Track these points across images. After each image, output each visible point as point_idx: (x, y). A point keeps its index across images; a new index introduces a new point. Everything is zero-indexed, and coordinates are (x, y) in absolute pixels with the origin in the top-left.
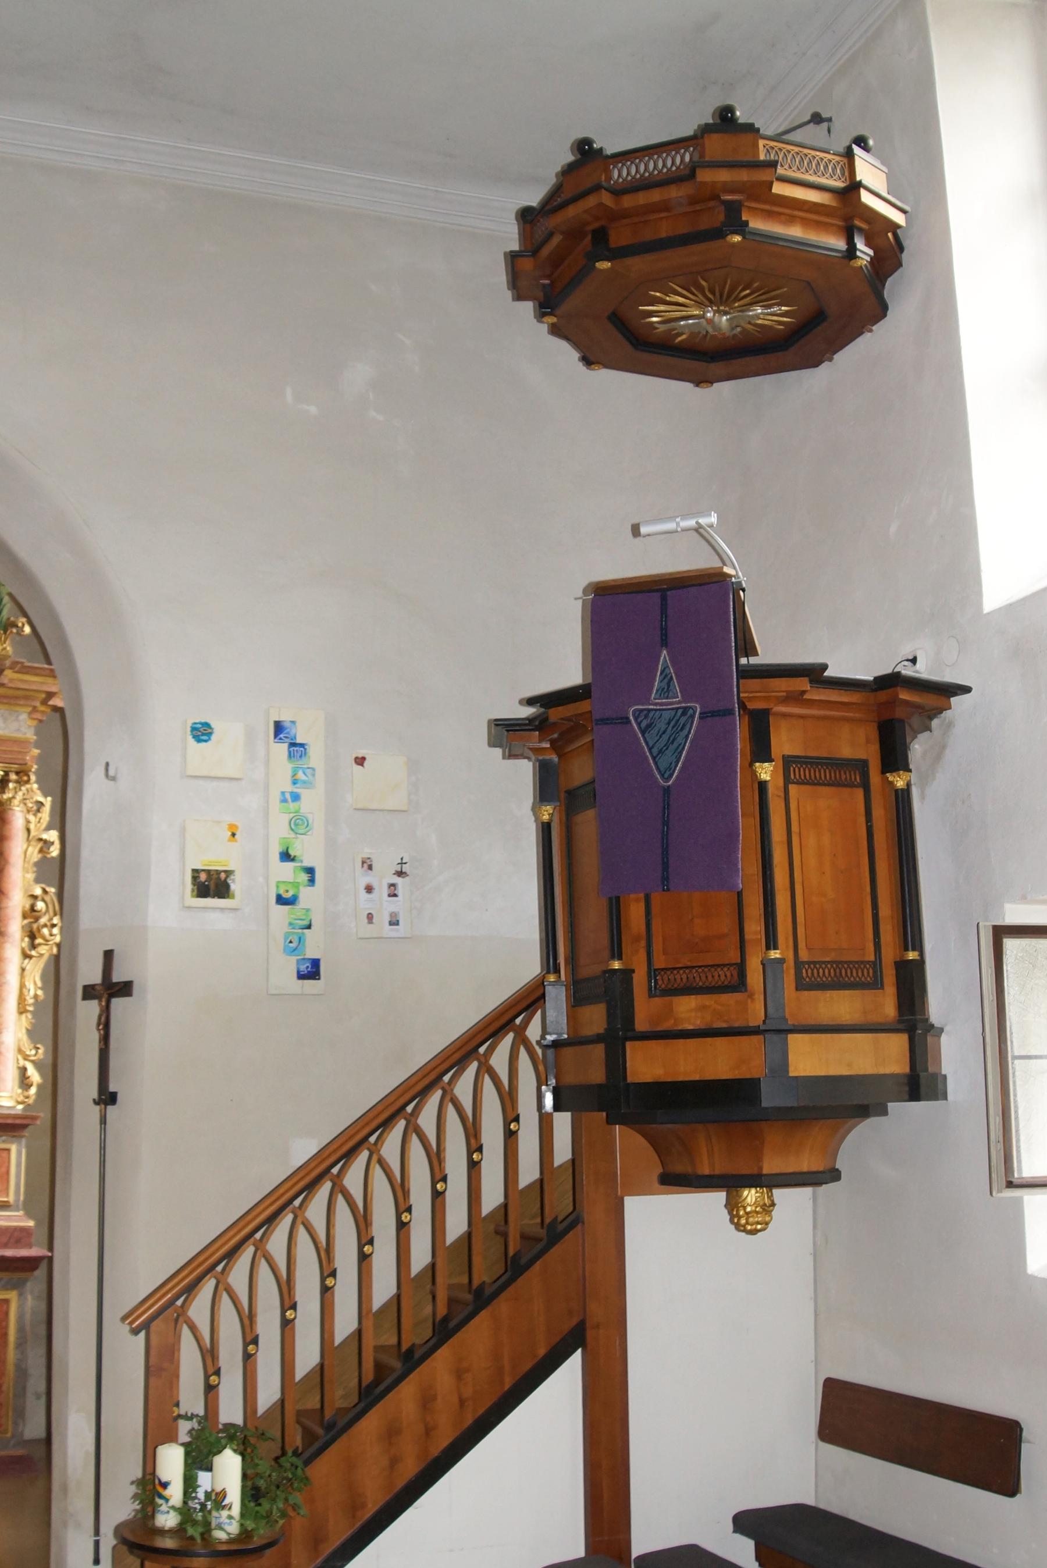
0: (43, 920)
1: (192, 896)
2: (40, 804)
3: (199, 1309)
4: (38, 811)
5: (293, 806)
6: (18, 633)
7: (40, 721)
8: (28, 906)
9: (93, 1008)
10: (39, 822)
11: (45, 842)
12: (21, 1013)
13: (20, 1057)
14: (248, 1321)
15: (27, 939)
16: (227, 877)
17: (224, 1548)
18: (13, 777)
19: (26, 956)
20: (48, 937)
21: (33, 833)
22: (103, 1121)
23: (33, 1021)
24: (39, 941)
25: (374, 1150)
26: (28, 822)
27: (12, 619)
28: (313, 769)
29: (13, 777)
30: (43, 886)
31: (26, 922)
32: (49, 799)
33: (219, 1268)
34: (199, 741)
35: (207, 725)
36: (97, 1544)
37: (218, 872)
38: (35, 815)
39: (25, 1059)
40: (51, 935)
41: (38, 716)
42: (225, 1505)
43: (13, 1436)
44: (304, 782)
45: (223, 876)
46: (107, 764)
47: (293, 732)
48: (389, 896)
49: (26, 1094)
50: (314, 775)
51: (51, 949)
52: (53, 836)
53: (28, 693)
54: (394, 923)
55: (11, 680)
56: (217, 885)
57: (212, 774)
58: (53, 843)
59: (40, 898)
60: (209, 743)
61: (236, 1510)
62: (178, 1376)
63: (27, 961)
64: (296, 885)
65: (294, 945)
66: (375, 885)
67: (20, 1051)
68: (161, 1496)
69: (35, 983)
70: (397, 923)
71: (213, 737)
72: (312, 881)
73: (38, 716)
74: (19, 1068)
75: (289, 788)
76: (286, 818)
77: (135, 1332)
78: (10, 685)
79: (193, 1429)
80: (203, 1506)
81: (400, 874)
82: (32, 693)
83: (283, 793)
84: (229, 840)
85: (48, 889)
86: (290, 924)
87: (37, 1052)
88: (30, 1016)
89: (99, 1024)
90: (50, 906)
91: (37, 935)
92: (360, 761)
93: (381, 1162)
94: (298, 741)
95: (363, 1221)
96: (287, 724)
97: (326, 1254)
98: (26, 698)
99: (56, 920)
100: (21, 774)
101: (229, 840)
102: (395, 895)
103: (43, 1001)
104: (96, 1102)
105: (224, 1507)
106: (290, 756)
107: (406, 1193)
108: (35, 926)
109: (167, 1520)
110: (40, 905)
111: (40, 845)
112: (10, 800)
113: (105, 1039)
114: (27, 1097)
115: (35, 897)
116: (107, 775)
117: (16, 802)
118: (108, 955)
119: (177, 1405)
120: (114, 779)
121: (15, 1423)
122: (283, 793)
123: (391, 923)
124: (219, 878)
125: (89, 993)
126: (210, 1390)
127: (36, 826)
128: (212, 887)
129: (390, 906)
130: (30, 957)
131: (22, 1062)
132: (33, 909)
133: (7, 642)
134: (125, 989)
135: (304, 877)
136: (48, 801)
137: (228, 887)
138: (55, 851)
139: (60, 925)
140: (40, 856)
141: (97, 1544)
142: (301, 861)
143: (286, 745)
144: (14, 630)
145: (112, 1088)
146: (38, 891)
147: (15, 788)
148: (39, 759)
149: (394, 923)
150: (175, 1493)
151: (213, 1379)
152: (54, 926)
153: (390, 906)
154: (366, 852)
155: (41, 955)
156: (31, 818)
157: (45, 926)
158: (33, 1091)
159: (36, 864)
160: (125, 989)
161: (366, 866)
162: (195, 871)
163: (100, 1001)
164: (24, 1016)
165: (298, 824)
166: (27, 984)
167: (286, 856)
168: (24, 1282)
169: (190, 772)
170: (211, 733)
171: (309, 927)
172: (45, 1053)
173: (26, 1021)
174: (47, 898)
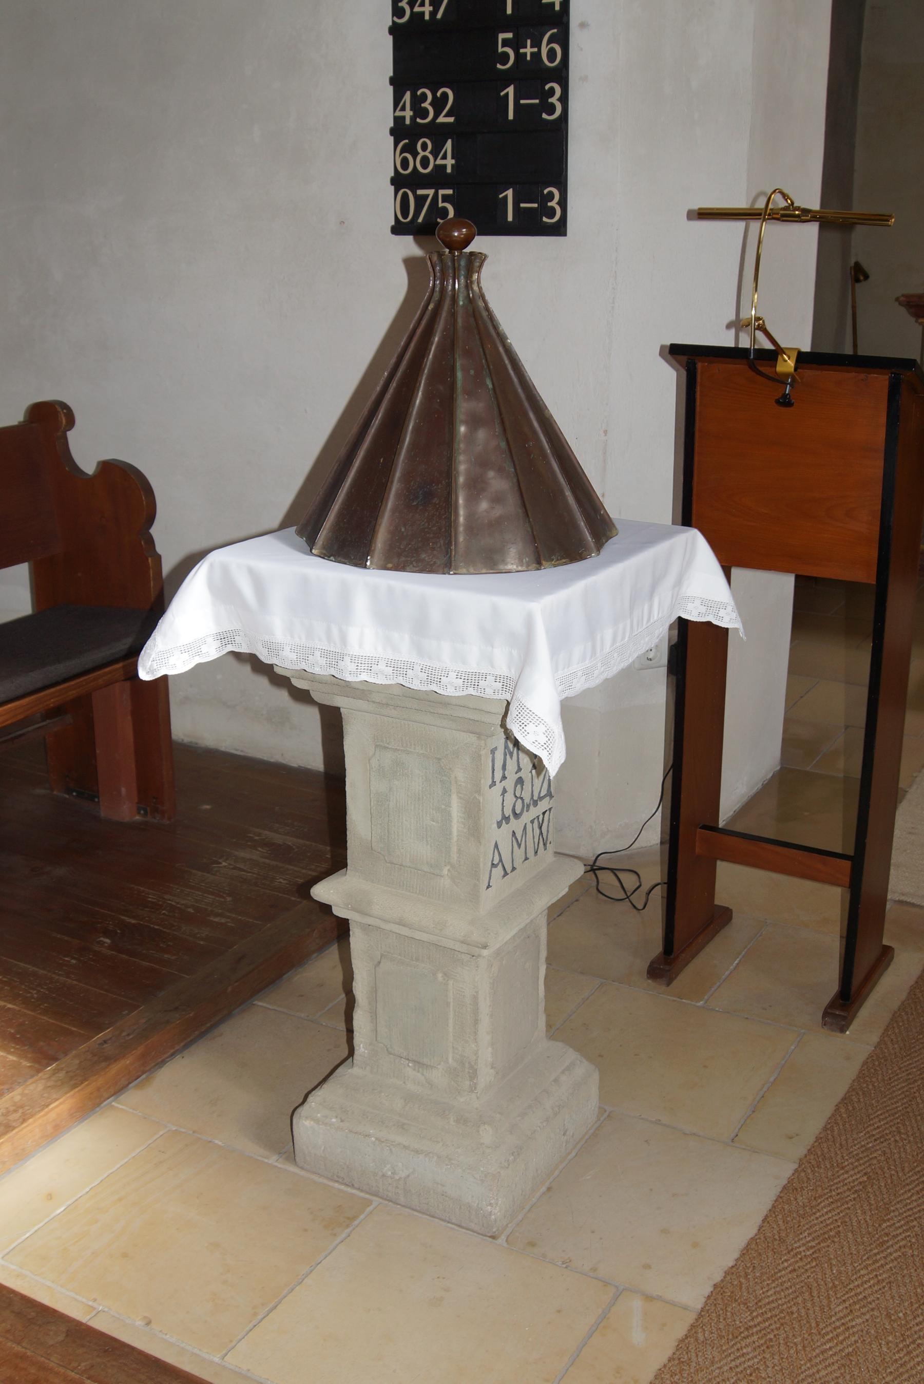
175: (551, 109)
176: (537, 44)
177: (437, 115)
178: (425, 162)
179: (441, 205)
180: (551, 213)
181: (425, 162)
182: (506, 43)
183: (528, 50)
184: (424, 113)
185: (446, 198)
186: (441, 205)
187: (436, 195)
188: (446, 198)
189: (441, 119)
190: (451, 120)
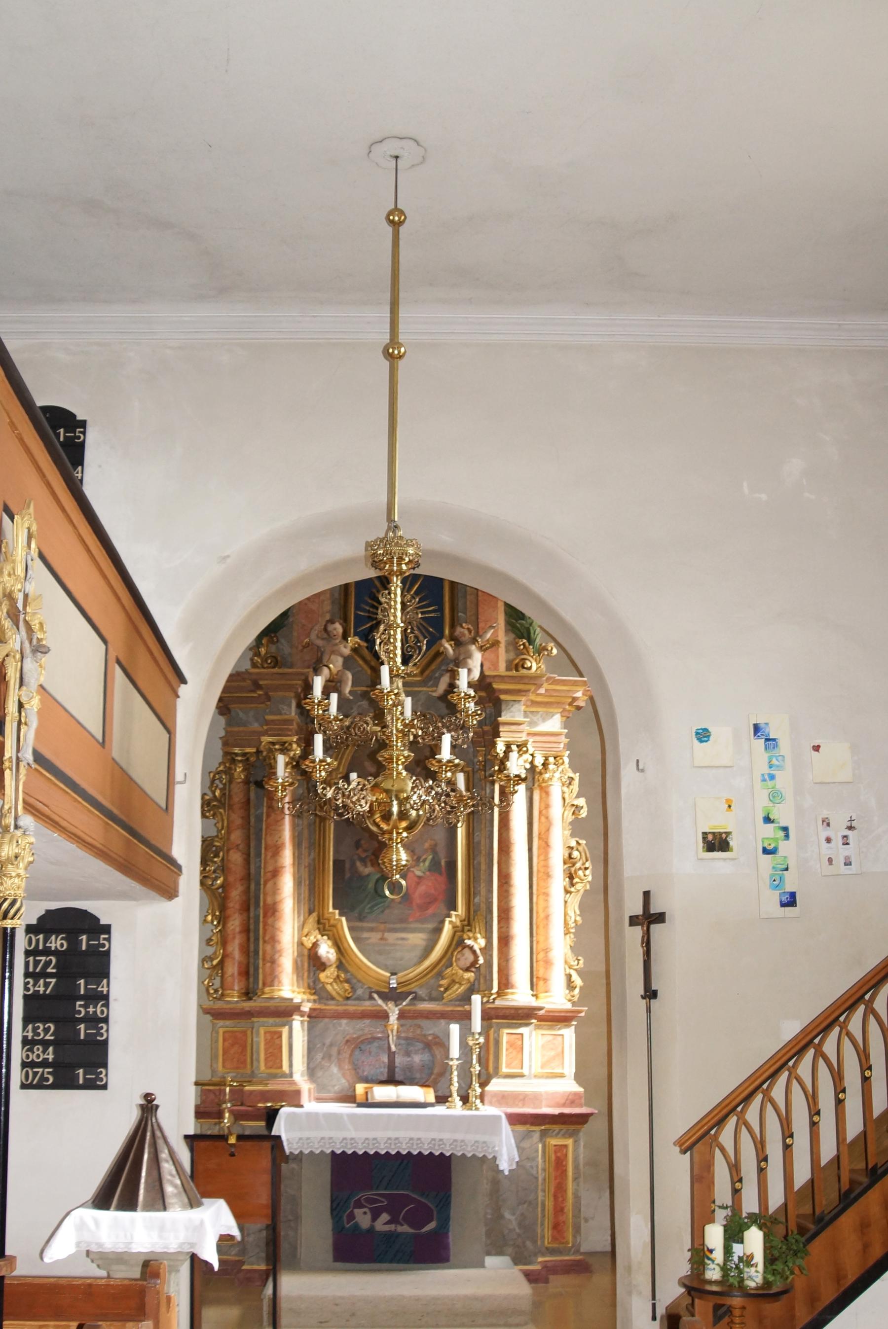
0: (578, 865)
1: (703, 851)
3: (726, 1136)
4: (570, 784)
5: (770, 784)
6: (548, 655)
7: (568, 717)
8: (567, 855)
9: (637, 932)
11: (577, 806)
12: (566, 934)
13: (567, 967)
14: (760, 1145)
15: (567, 879)
16: (727, 836)
17: (752, 1292)
18: (551, 760)
19: (567, 892)
20: (583, 877)
22: (649, 1010)
23: (575, 939)
25: (844, 1026)
26: (563, 793)
27: (544, 644)
28: (783, 756)
29: (551, 760)
30: (577, 839)
31: (566, 866)
32: (578, 774)
33: (739, 1109)
34: (701, 742)
35: (706, 730)
36: (654, 1305)
37: (720, 833)
38: (568, 787)
39: (570, 968)
40: (585, 876)
41: (566, 714)
42: (753, 1265)
43: (572, 1247)
44: (778, 766)
45: (724, 836)
46: (638, 761)
47: (767, 730)
48: (844, 844)
49: (572, 994)
50: (783, 760)
51: (585, 885)
52: (581, 802)
54: (848, 863)
56: (720, 843)
57: (712, 764)
58: (582, 807)
60: (709, 742)
61: (761, 1267)
62: (713, 1183)
63: (568, 895)
64: (776, 840)
65: (777, 883)
66: (833, 837)
67: (566, 962)
68: (709, 1259)
69: (575, 912)
70: (850, 864)
71: (711, 738)
72: (787, 836)
73: (566, 714)
74: (566, 975)
75: (766, 770)
76: (766, 793)
77: (684, 1152)
79: (728, 1215)
80: (737, 1267)
81: (850, 828)
83: (763, 775)
84: (727, 811)
85: (580, 841)
86: (773, 868)
87: (578, 963)
88: (572, 936)
89: (642, 943)
90: (583, 854)
92: (817, 748)
93: (849, 1034)
94: (771, 737)
95: (838, 1076)
96: (762, 726)
97: (812, 1099)
99: (587, 865)
100: (558, 759)
101: (727, 811)
102: (848, 844)
103: (581, 925)
104: (643, 997)
105: (752, 1265)
106: (766, 748)
107: (867, 1057)
109: (713, 1273)
110: (576, 854)
111: (574, 808)
113: (647, 953)
114: (573, 996)
115: (571, 848)
116: (638, 769)
117: (555, 779)
118: (647, 895)
119: (714, 1202)
120: (643, 771)
121: (574, 1237)
122: (763, 775)
123: (846, 864)
124: (721, 838)
125: (634, 921)
126: (736, 1192)
128: (717, 844)
129: (844, 851)
130: (571, 893)
131: (568, 971)
132: (570, 857)
133: (542, 661)
134: (660, 918)
135: (781, 834)
136: (577, 777)
137: (728, 843)
138: (584, 813)
139: (591, 867)
140: (574, 817)
141: (654, 1305)
142: (779, 823)
143: (763, 740)
144: (546, 653)
145: (653, 988)
146: (573, 843)
148: (568, 747)
149: (848, 863)
150: (718, 1255)
151: (738, 1185)
152: (586, 869)
153: (844, 851)
154: (825, 814)
155: (578, 891)
156: (565, 789)
157: (580, 869)
158: (577, 991)
159: (571, 823)
160: (660, 918)
161: (825, 823)
162: (704, 833)
163: (643, 927)
164: (568, 936)
165: (775, 796)
166: (569, 912)
167: (768, 820)
168: (578, 1131)
169: (695, 765)
170: (709, 736)
171: (787, 869)
172: (584, 963)
173: (569, 940)
174: (580, 848)
175: (102, 1035)
176: (95, 1007)
177: (45, 1035)
178: (38, 1056)
179: (45, 1076)
180: (102, 1080)
181: (38, 1056)
182: (80, 1006)
183: (91, 1010)
184: (39, 1034)
185: (49, 1073)
186: (46, 1076)
187: (43, 1072)
188: (49, 1073)
189: (47, 1037)
190: (52, 1038)
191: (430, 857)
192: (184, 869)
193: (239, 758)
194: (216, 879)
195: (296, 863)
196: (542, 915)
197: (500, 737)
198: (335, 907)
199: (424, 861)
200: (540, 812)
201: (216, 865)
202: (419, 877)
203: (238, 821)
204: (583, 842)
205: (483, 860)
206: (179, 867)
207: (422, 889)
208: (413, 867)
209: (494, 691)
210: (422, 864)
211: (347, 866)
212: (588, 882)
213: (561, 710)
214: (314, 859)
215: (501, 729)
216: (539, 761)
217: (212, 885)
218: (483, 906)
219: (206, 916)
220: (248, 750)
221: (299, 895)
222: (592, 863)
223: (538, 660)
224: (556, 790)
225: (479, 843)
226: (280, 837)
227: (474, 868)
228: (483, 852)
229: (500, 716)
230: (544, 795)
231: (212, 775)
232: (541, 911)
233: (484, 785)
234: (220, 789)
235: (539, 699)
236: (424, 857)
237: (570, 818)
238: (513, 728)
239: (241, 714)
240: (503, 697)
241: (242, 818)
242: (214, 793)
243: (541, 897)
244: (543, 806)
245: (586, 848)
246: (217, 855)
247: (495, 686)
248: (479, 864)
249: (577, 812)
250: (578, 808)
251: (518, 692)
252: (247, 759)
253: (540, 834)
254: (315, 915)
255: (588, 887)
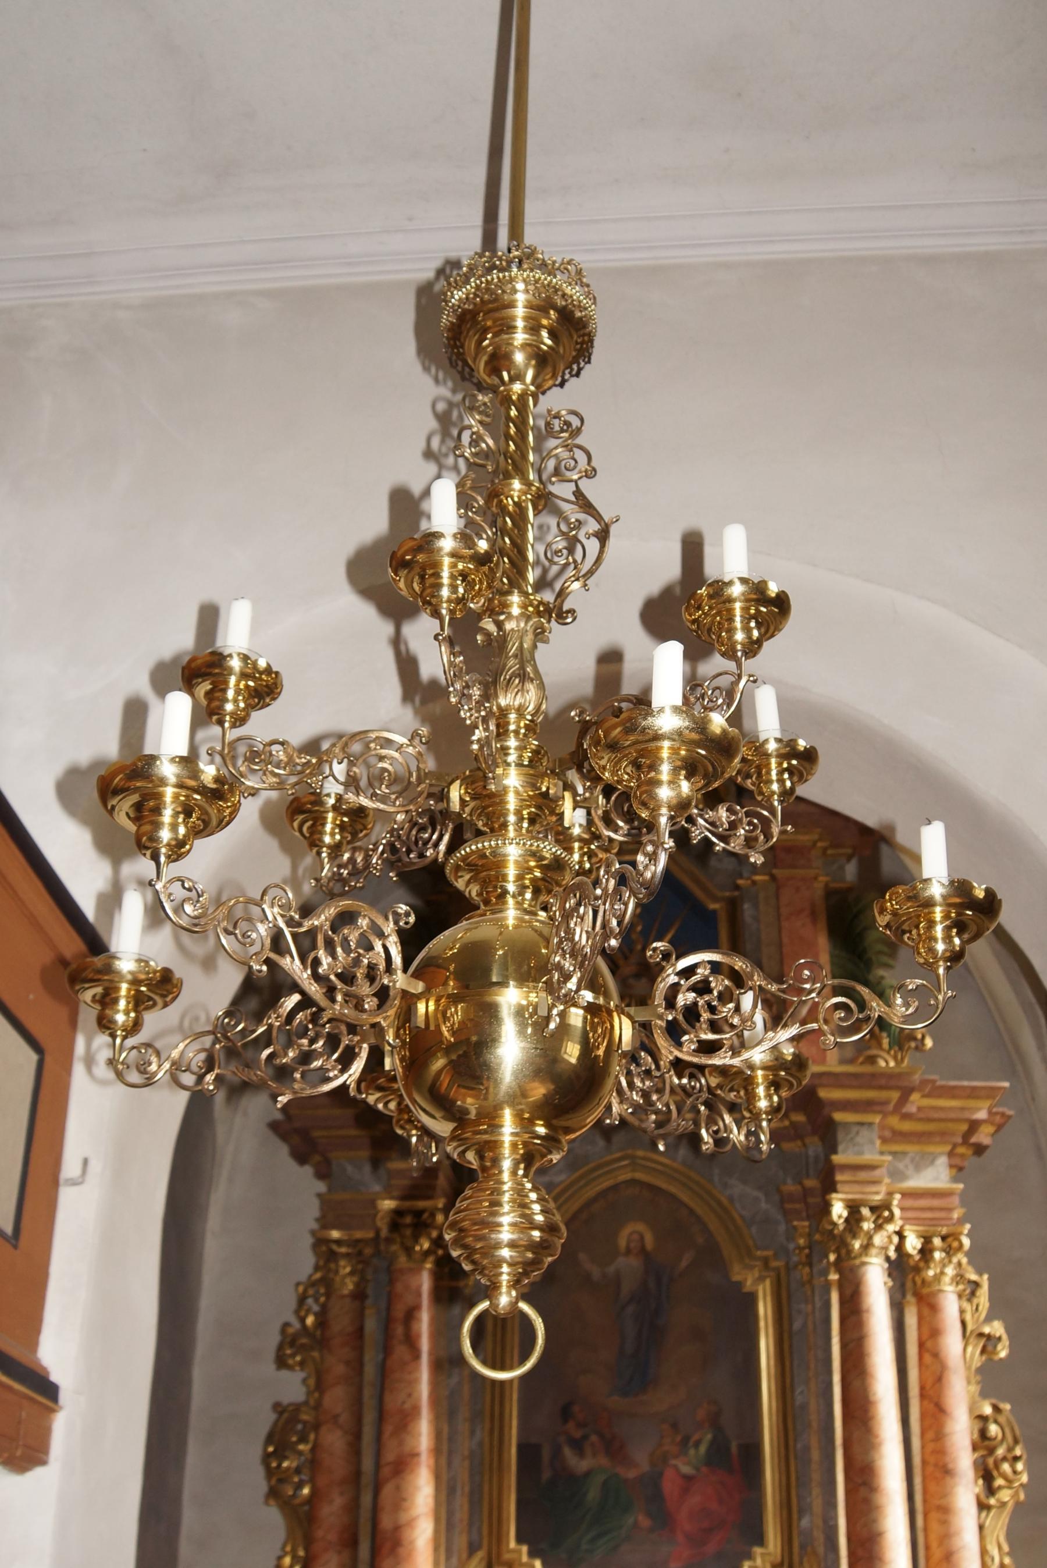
0: (1000, 1452)
2: (976, 1285)
4: (973, 1294)
6: (917, 1048)
10: (977, 1309)
11: (989, 1337)
15: (981, 1482)
18: (937, 1241)
19: (982, 1506)
21: (970, 1327)
24: (999, 1482)
26: (962, 1312)
29: (937, 1241)
30: (994, 1401)
32: (986, 1277)
38: (969, 1300)
40: (1015, 1472)
41: (957, 1161)
52: (996, 1328)
53: (942, 1126)
55: (919, 1109)
58: (999, 1339)
59: (991, 1420)
63: (984, 1514)
73: (957, 1161)
78: (921, 1115)
82: (950, 1125)
85: (1002, 1406)
91: (995, 1473)
98: (943, 1134)
99: (1018, 1452)
100: (950, 1240)
108: (991, 1461)
110: (993, 1429)
112: (938, 1277)
115: (983, 1419)
117: (947, 1279)
127: (973, 1315)
132: (983, 1434)
139: (1025, 1457)
140: (984, 1358)
144: (913, 1044)
146: (988, 1410)
147: (942, 1260)
152: (1016, 1459)
155: (1003, 1504)
156: (967, 1306)
157: (1004, 1459)
159: (979, 1370)
166: (989, 1547)
174: (1002, 1419)
191: (709, 1437)
192: (64, 1397)
193: (343, 1250)
194: (300, 1486)
195: (445, 1448)
196: (937, 1553)
197: (835, 1191)
198: (520, 1540)
199: (697, 1444)
200: (921, 1345)
201: (303, 1458)
202: (688, 1478)
203: (338, 1368)
204: (1007, 1407)
205: (814, 1442)
206: (49, 1390)
207: (695, 1500)
208: (676, 1457)
209: (820, 1103)
210: (692, 1452)
211: (546, 1454)
212: (1022, 1485)
213: (948, 1148)
214: (481, 1444)
215: (839, 1177)
216: (913, 1244)
217: (294, 1496)
218: (819, 1536)
219: (280, 1558)
220: (359, 1235)
221: (450, 1514)
222: (1027, 1448)
223: (899, 1057)
224: (950, 1305)
225: (804, 1407)
226: (410, 1395)
227: (796, 1458)
228: (815, 1424)
229: (835, 1152)
230: (926, 1311)
231: (301, 1289)
232: (934, 1545)
233: (809, 1293)
234: (316, 1315)
235: (907, 1126)
236: (696, 1437)
237: (977, 1360)
238: (863, 1175)
239: (350, 1169)
240: (838, 1116)
241: (347, 1363)
242: (302, 1320)
243: (934, 1515)
244: (926, 1332)
245: (1012, 1419)
246: (303, 1439)
247: (823, 1093)
248: (807, 1449)
249: (990, 1348)
250: (989, 1342)
251: (867, 1106)
252: (360, 1253)
253: (922, 1388)
254: (481, 1554)
255: (1022, 1496)
